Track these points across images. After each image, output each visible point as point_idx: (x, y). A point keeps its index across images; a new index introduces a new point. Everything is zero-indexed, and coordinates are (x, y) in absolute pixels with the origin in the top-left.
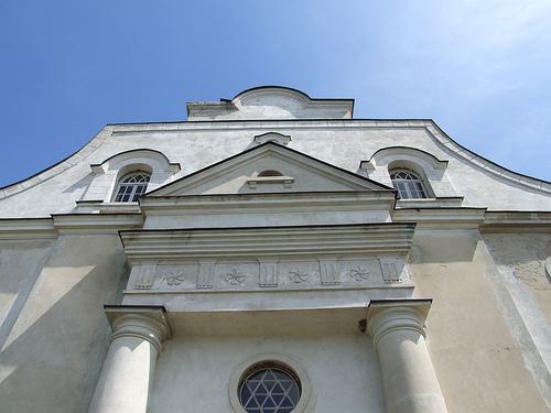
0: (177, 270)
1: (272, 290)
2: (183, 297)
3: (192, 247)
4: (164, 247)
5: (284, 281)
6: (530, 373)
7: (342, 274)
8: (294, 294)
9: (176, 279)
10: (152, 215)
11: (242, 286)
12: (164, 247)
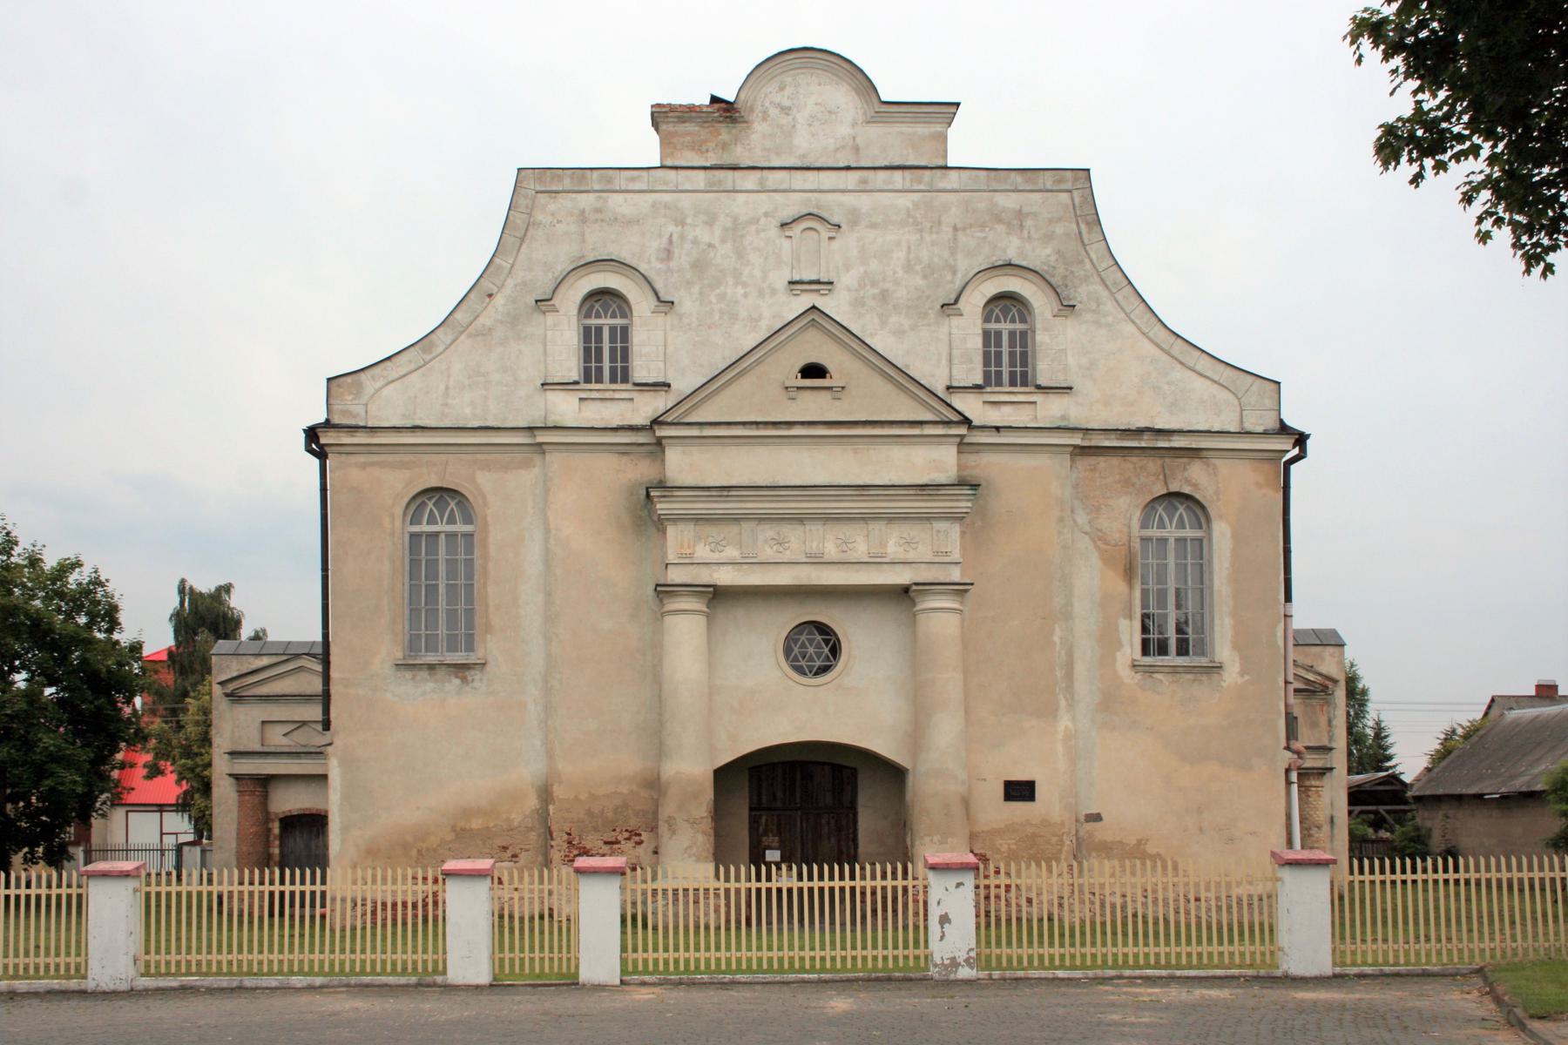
0: (713, 531)
1: (818, 561)
2: (730, 567)
3: (732, 507)
4: (701, 507)
5: (831, 550)
6: (1055, 644)
7: (891, 542)
8: (840, 565)
9: (717, 546)
11: (788, 556)
12: (701, 507)
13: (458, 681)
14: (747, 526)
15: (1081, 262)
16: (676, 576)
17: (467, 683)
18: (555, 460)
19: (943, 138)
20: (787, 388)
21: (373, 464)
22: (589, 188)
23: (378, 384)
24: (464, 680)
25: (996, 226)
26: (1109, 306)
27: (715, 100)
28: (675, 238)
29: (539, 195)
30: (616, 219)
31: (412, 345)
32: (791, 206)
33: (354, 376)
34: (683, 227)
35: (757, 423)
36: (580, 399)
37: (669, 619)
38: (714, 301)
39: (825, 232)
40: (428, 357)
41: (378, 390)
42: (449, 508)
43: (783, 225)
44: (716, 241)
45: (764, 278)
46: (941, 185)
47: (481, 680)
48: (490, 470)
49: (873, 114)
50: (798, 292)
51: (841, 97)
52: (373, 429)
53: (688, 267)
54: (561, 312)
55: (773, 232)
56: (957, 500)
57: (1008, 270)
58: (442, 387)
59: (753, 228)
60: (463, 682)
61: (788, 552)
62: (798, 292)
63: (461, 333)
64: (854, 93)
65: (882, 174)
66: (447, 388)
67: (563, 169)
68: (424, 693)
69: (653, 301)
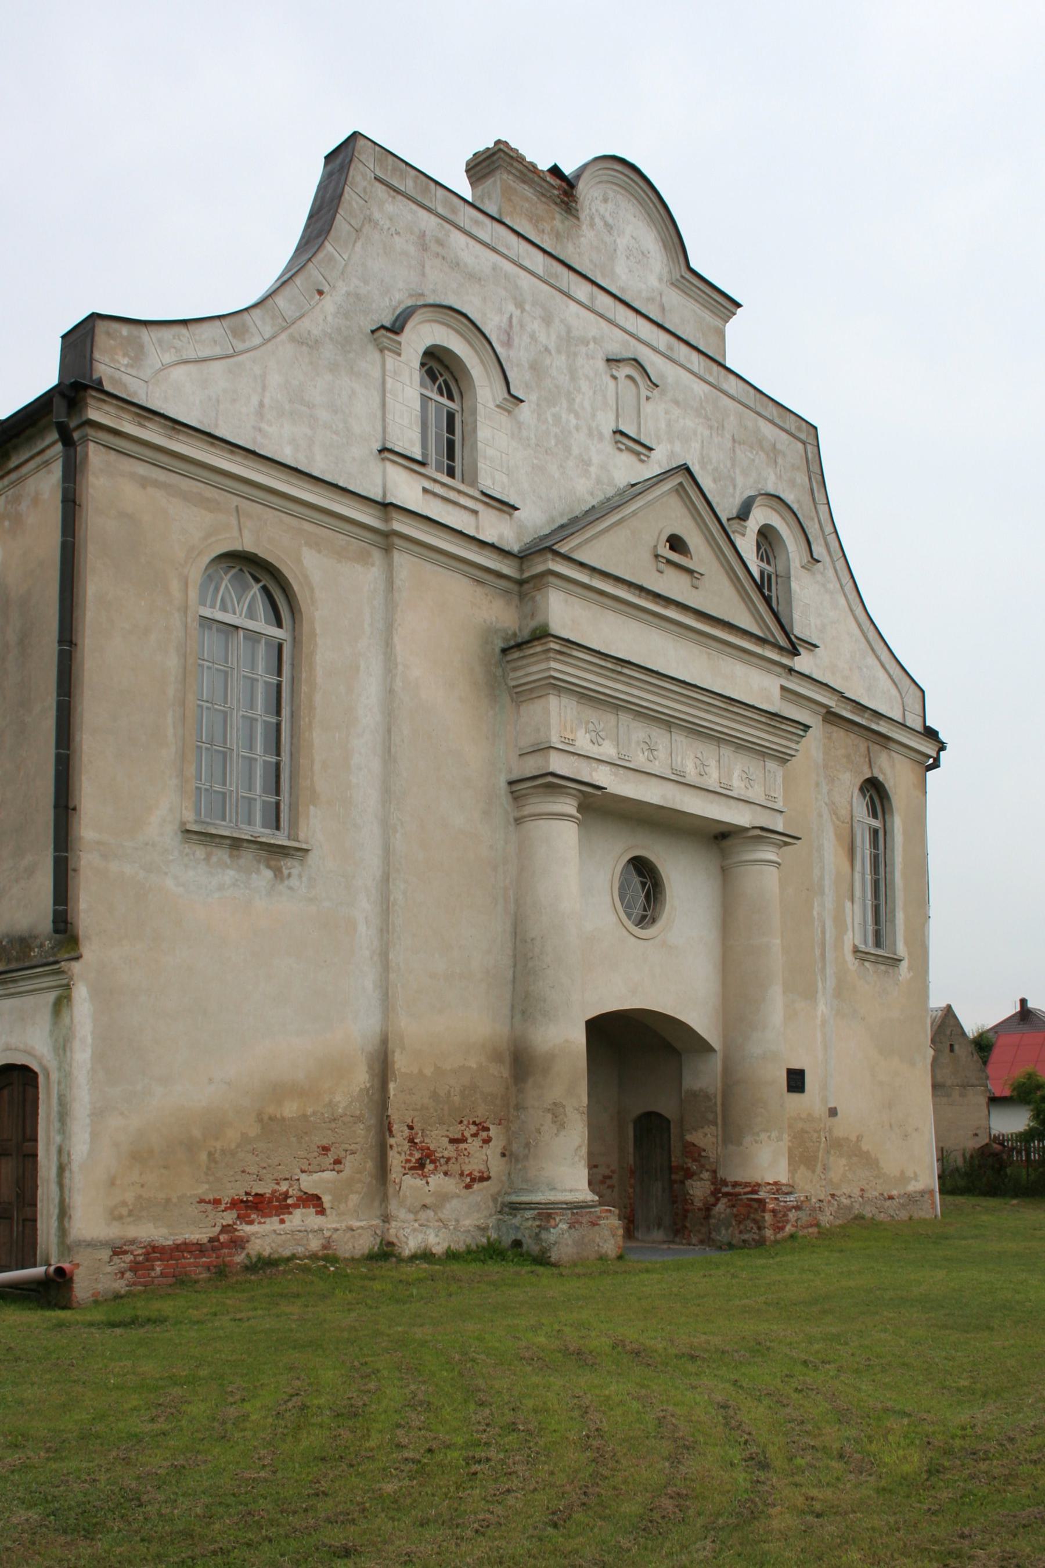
8: (698, 792)
10: (557, 588)
11: (655, 768)
13: (268, 874)
14: (625, 718)
15: (813, 519)
16: (559, 764)
17: (282, 880)
18: (404, 562)
19: (721, 335)
20: (657, 556)
21: (156, 484)
22: (429, 205)
23: (168, 358)
24: (278, 874)
25: (760, 453)
26: (830, 573)
27: (555, 171)
28: (515, 321)
29: (377, 184)
30: (458, 264)
31: (219, 317)
32: (617, 344)
33: (134, 330)
34: (522, 312)
35: (641, 589)
36: (425, 490)
37: (530, 826)
38: (550, 420)
39: (644, 392)
40: (240, 346)
41: (165, 367)
42: (252, 593)
43: (608, 360)
44: (552, 346)
45: (594, 416)
46: (725, 386)
47: (300, 876)
48: (319, 552)
49: (678, 277)
50: (623, 447)
51: (649, 240)
52: (176, 425)
53: (527, 366)
54: (403, 358)
55: (601, 364)
56: (790, 740)
57: (774, 503)
58: (255, 400)
59: (583, 349)
60: (276, 876)
61: (657, 763)
62: (623, 447)
63: (284, 329)
64: (661, 244)
65: (684, 349)
66: (261, 405)
67: (407, 164)
68: (221, 888)
69: (501, 393)
